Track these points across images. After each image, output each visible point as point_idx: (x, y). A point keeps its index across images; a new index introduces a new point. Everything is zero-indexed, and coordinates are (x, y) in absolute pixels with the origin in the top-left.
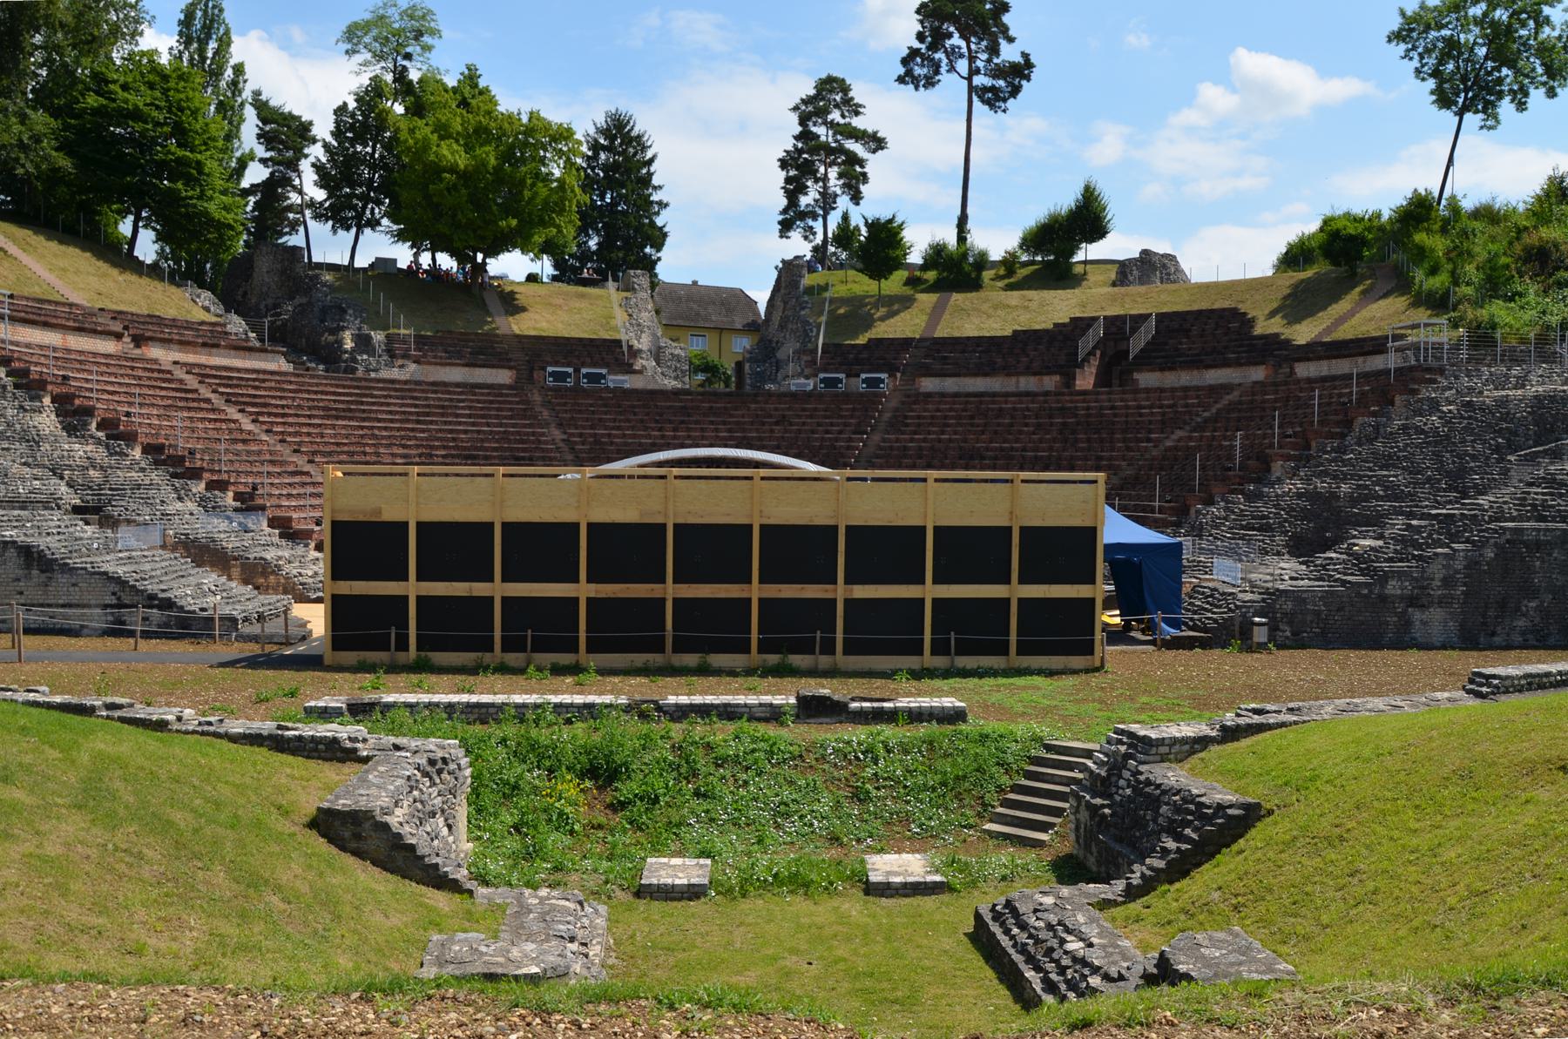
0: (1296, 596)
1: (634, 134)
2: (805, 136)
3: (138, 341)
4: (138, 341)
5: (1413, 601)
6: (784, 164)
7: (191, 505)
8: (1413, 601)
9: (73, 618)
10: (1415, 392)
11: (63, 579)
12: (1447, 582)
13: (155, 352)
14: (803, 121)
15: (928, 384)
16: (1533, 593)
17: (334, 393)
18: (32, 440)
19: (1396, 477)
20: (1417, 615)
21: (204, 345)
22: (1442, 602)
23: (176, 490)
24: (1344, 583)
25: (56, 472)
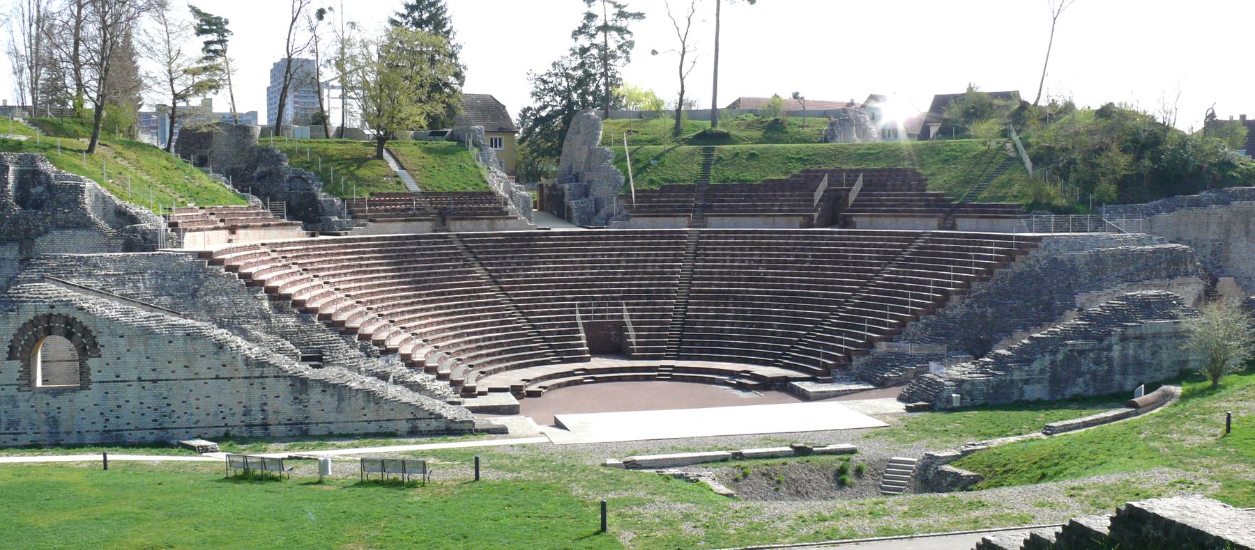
0: (973, 383)
3: (233, 230)
4: (233, 230)
5: (1026, 382)
6: (576, 34)
7: (358, 353)
8: (1026, 382)
9: (391, 427)
11: (386, 407)
12: (1042, 371)
15: (716, 224)
16: (1080, 375)
17: (345, 254)
18: (265, 317)
21: (264, 226)
22: (1039, 382)
23: (347, 343)
24: (993, 375)
25: (283, 336)
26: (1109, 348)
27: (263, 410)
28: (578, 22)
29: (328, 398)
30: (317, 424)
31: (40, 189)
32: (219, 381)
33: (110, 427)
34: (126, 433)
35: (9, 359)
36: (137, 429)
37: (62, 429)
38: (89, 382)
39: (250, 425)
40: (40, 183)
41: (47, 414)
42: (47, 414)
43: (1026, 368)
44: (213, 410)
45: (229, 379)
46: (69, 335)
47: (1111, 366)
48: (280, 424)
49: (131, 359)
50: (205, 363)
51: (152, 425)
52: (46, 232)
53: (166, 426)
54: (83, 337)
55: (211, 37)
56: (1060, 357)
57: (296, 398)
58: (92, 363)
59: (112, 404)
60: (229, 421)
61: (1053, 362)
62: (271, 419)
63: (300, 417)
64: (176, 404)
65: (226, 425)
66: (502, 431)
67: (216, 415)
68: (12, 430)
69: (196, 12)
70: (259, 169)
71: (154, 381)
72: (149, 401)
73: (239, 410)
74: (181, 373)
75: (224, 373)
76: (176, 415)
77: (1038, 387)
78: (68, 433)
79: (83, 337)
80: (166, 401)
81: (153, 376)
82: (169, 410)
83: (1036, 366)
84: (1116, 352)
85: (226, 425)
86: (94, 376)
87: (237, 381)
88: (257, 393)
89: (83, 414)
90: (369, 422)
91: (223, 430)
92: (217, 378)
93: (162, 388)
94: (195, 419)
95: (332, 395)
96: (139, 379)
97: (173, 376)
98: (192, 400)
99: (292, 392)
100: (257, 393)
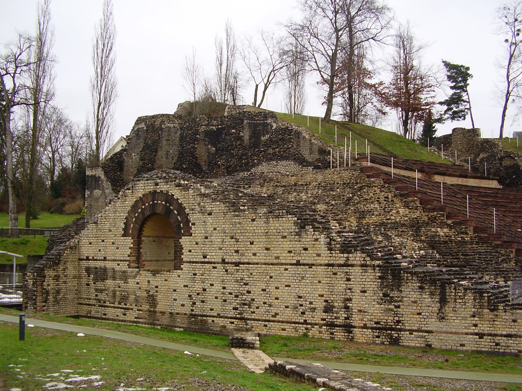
27: (347, 308)
29: (427, 299)
30: (411, 331)
32: (301, 269)
33: (197, 312)
34: (210, 320)
35: (124, 236)
36: (219, 316)
37: (159, 308)
38: (182, 262)
39: (331, 325)
41: (148, 292)
42: (148, 292)
44: (292, 301)
45: (311, 266)
48: (365, 327)
49: (216, 238)
50: (287, 245)
51: (232, 314)
52: (258, 165)
53: (246, 315)
54: (179, 214)
57: (385, 295)
59: (198, 287)
60: (308, 316)
62: (356, 320)
63: (390, 319)
64: (256, 289)
65: (305, 322)
68: (123, 305)
71: (237, 264)
72: (232, 287)
73: (320, 304)
74: (261, 258)
75: (306, 258)
76: (255, 304)
78: (163, 313)
79: (179, 214)
80: (247, 288)
81: (236, 258)
82: (249, 298)
85: (305, 322)
86: (186, 256)
87: (320, 269)
88: (341, 285)
89: (175, 295)
90: (481, 336)
91: (302, 329)
92: (298, 264)
93: (243, 273)
94: (274, 310)
95: (432, 294)
96: (223, 262)
97: (255, 260)
98: (271, 289)
99: (382, 287)
100: (341, 285)
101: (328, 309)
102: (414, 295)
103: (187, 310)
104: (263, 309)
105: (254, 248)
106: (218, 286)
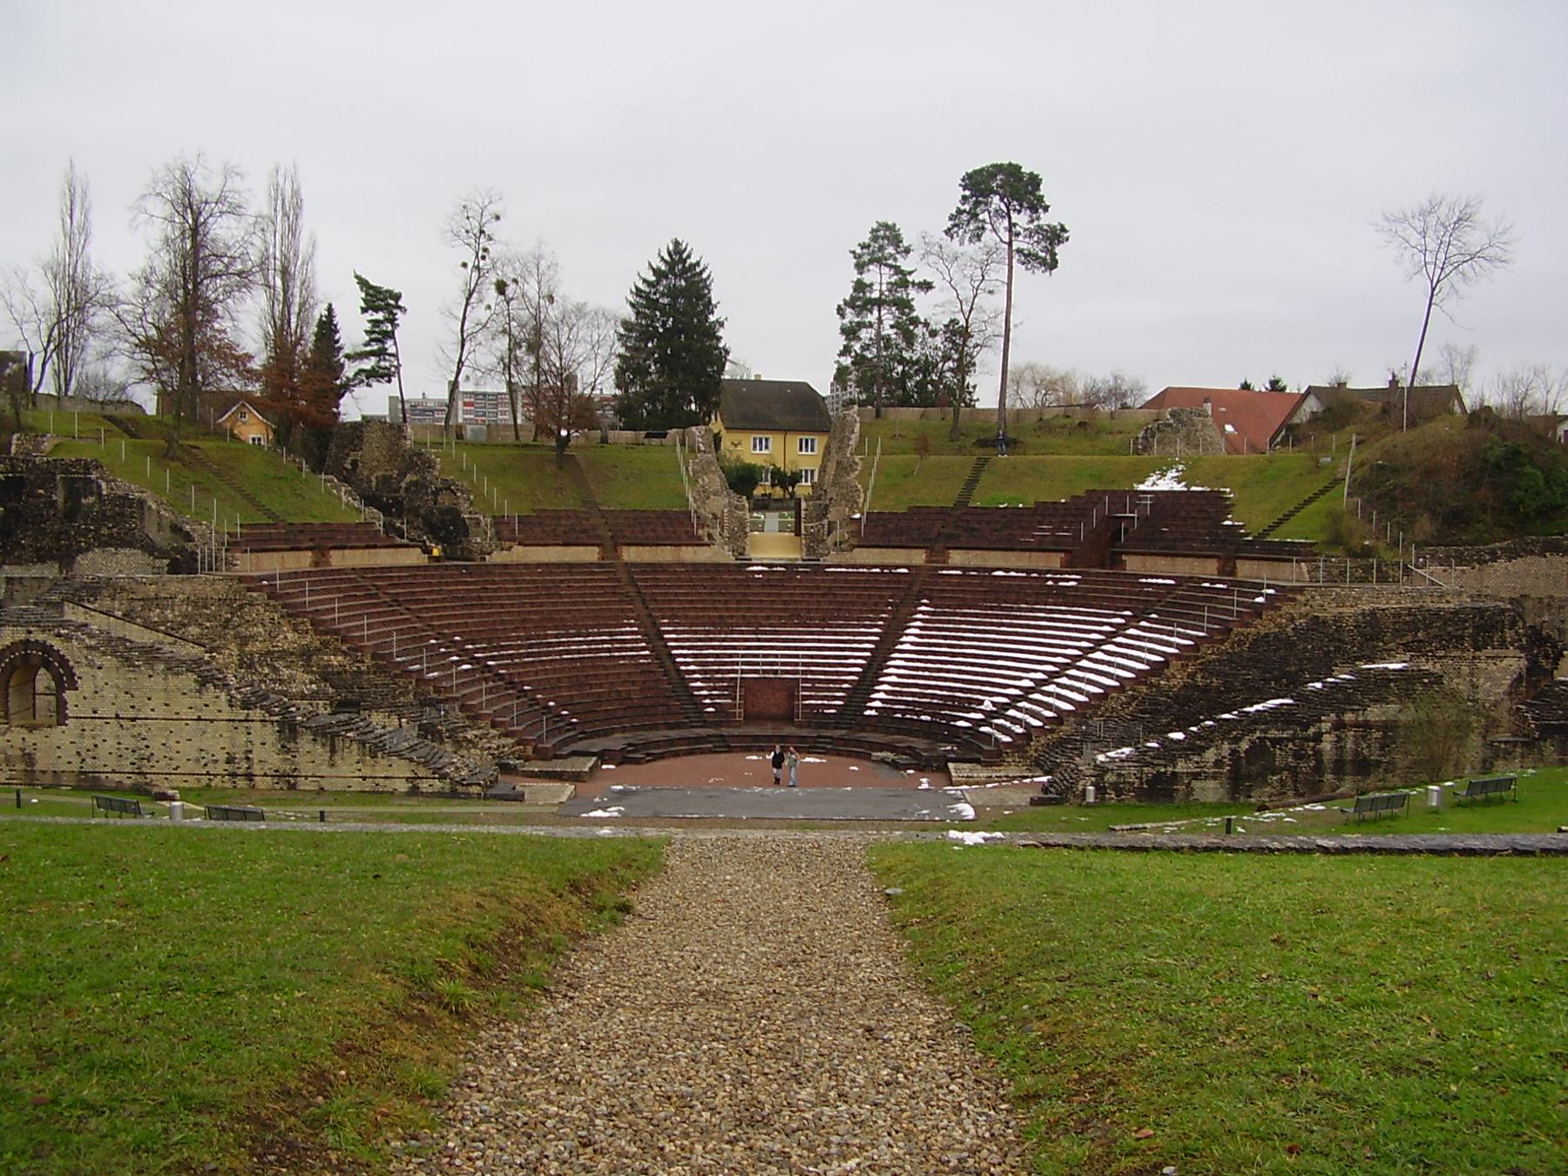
1: (693, 260)
2: (860, 286)
5: (1196, 776)
8: (1196, 776)
10: (1279, 608)
12: (1218, 763)
13: (338, 559)
14: (860, 267)
19: (1252, 674)
20: (1196, 784)
26: (1318, 738)
28: (848, 292)
31: (91, 499)
36: (114, 772)
37: (38, 767)
39: (234, 775)
40: (92, 494)
41: (23, 750)
42: (23, 750)
43: (1196, 758)
44: (195, 754)
46: (47, 665)
47: (1319, 762)
49: (109, 693)
50: (188, 701)
52: (87, 550)
55: (380, 316)
56: (1244, 745)
58: (69, 695)
59: (88, 743)
61: (1234, 752)
62: (256, 769)
63: (288, 768)
64: (155, 747)
66: (519, 798)
67: (197, 760)
69: (363, 283)
70: (409, 478)
71: (133, 720)
72: (128, 742)
73: (222, 756)
74: (161, 712)
76: (155, 758)
77: (1211, 784)
78: (44, 772)
81: (132, 714)
83: (1210, 755)
84: (1327, 745)
89: (59, 753)
90: (364, 778)
91: (205, 780)
92: (199, 719)
93: (139, 727)
95: (324, 745)
96: (117, 717)
98: (171, 743)
101: (230, 760)
102: (309, 747)
103: (75, 767)
104: (163, 763)
105: (152, 704)
106: (111, 742)
